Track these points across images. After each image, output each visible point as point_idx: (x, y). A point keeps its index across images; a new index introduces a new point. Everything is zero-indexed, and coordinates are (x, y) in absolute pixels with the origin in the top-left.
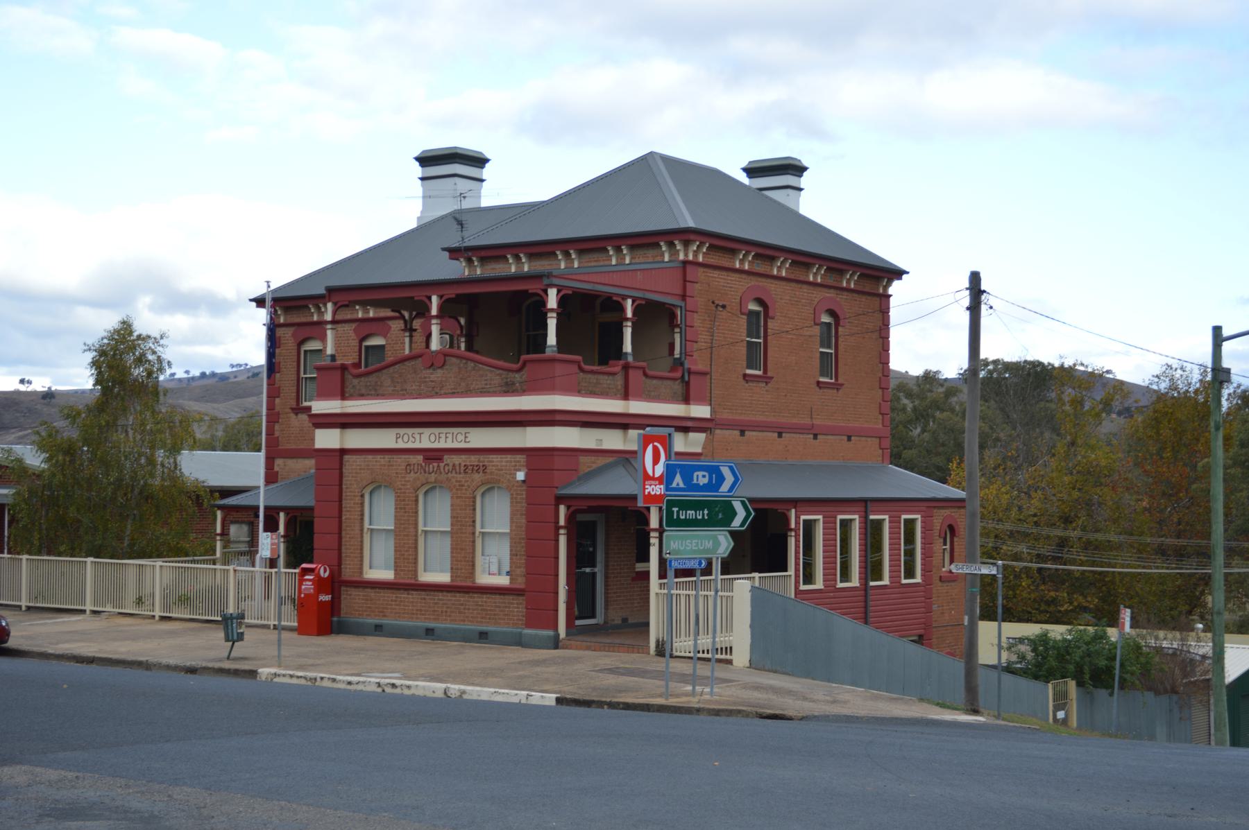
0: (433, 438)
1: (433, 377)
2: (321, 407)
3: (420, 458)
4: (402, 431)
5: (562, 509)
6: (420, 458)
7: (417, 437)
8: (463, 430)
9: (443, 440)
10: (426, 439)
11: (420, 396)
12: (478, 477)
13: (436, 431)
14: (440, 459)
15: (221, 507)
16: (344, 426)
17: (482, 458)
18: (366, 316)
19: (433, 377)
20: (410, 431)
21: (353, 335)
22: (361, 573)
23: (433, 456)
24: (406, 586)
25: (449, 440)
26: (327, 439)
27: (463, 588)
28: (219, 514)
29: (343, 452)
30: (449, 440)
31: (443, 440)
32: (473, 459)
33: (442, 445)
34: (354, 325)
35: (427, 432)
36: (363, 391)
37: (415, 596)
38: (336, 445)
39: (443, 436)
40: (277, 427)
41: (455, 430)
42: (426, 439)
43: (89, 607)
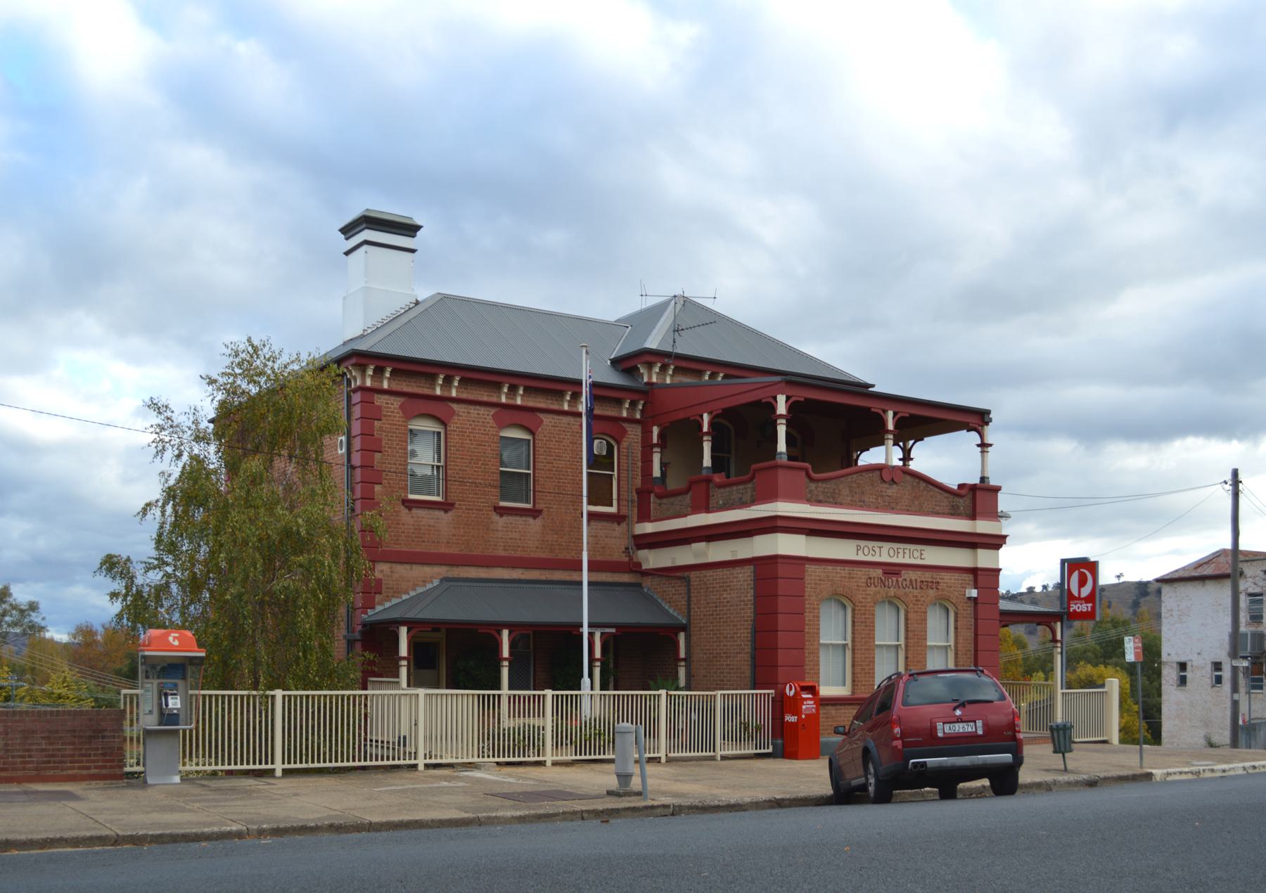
1: (889, 492)
3: (878, 572)
6: (878, 572)
7: (877, 550)
8: (919, 547)
9: (901, 555)
11: (877, 508)
12: (932, 593)
13: (895, 546)
14: (898, 574)
19: (889, 492)
20: (870, 544)
21: (490, 419)
23: (892, 570)
25: (907, 556)
30: (907, 556)
31: (901, 555)
35: (886, 546)
41: (912, 547)
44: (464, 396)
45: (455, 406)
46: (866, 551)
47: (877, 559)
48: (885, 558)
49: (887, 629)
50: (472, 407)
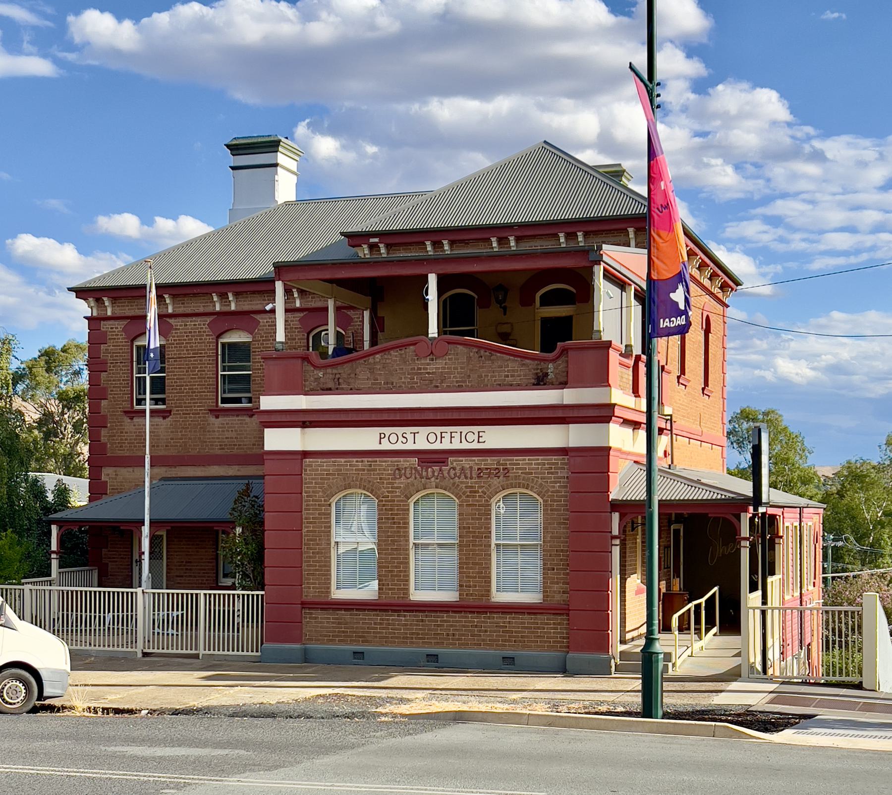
0: (432, 438)
1: (432, 368)
2: (268, 403)
3: (414, 461)
4: (387, 430)
5: (616, 517)
6: (414, 461)
7: (410, 437)
10: (422, 439)
13: (438, 430)
14: (444, 462)
15: (55, 522)
16: (304, 425)
17: (502, 459)
18: (226, 309)
19: (432, 368)
22: (328, 592)
23: (432, 458)
24: (393, 605)
26: (277, 440)
27: (474, 606)
28: (54, 528)
29: (305, 454)
32: (490, 460)
33: (446, 445)
34: (209, 320)
35: (423, 431)
36: (331, 385)
37: (407, 618)
38: (298, 447)
39: (447, 436)
40: (104, 432)
41: (465, 429)
42: (422, 439)
43: (202, 652)
44: (181, 310)
45: (172, 321)
46: (393, 438)
47: (410, 446)
48: (422, 444)
49: (433, 524)
50: (189, 319)
